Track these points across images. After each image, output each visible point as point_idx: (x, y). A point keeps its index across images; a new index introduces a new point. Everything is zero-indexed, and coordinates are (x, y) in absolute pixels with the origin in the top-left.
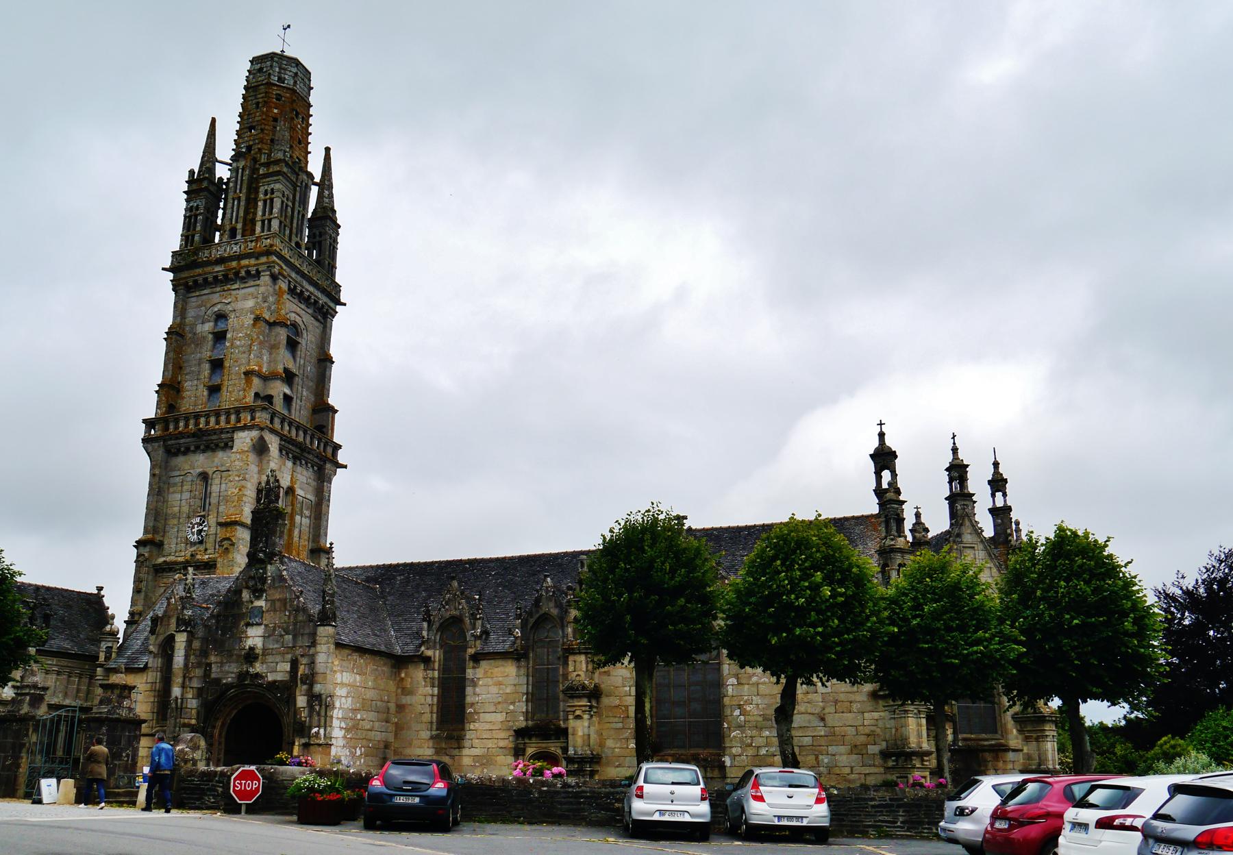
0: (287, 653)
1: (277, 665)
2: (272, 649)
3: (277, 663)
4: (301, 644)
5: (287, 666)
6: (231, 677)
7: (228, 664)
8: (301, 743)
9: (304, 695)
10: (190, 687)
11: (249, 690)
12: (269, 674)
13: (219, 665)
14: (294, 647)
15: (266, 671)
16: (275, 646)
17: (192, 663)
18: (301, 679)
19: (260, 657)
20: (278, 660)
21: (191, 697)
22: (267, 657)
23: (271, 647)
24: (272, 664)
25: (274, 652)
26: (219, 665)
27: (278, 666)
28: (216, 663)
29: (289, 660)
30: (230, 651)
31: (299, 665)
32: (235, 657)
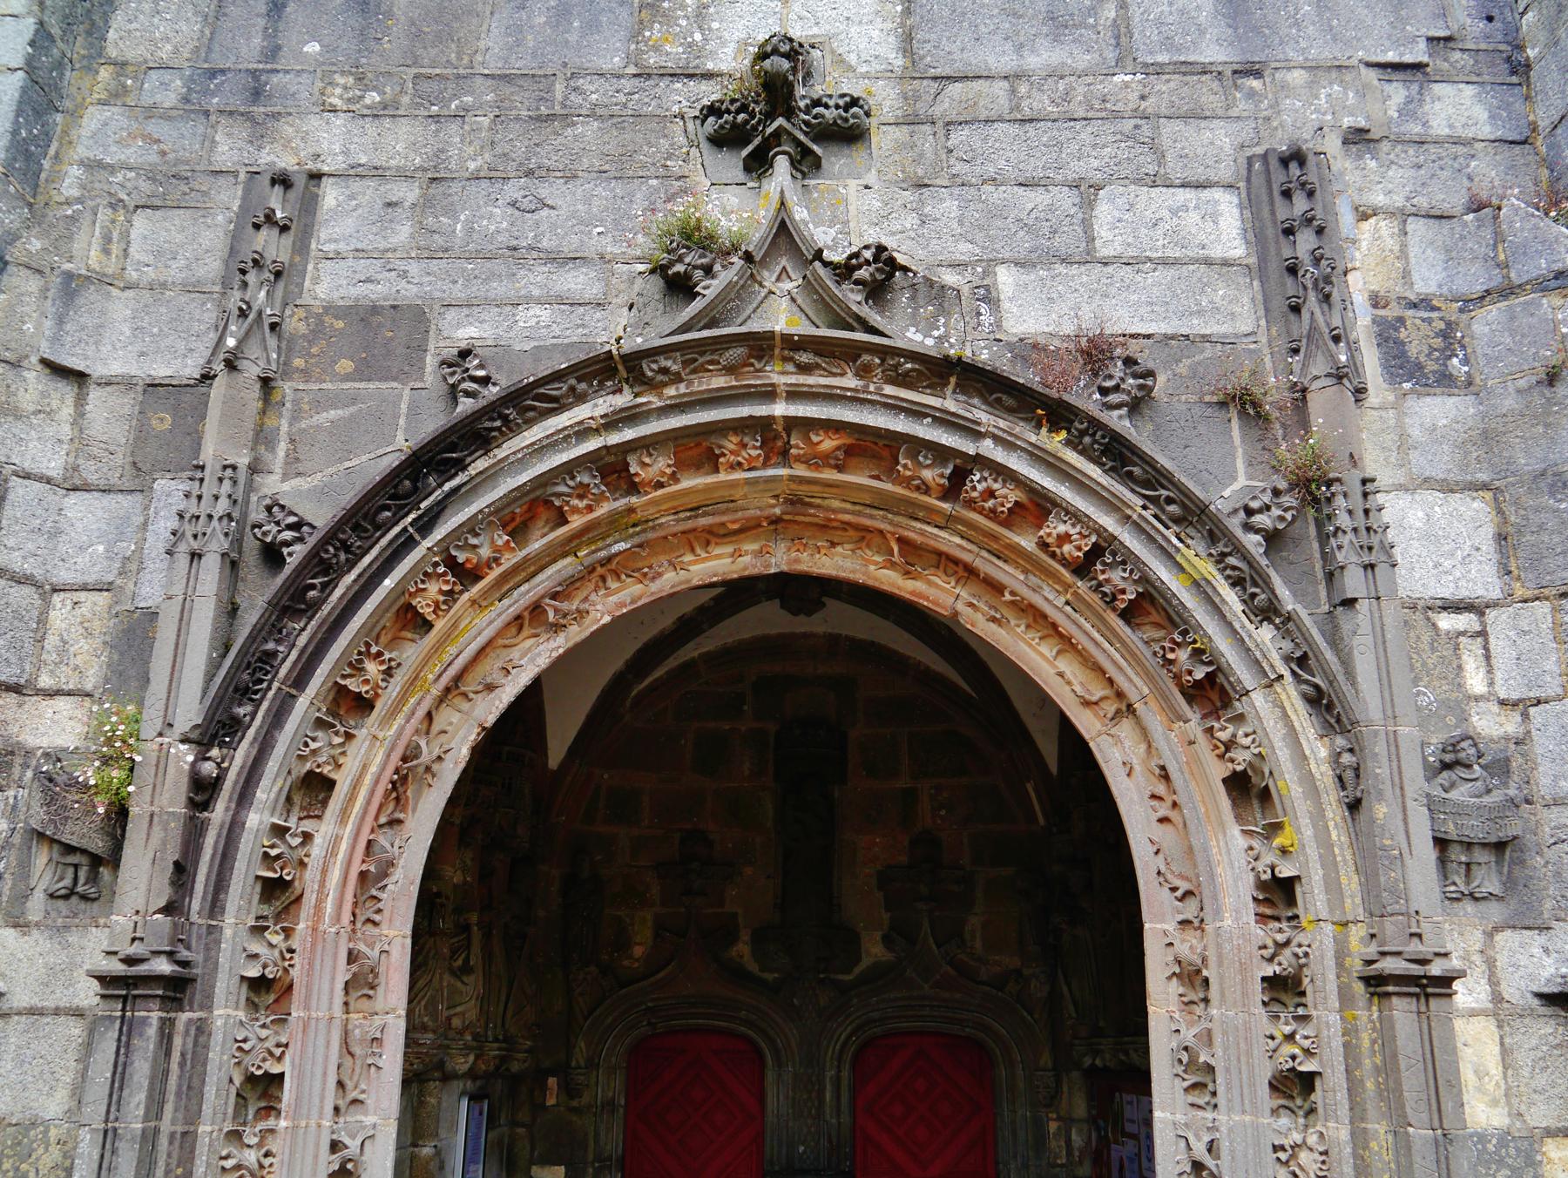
0: (1196, 115)
1: (1088, 204)
2: (1013, 77)
3: (1088, 191)
4: (1321, 51)
5: (1215, 217)
6: (560, 300)
7: (513, 190)
8: (1517, 989)
9: (1447, 488)
10: (58, 370)
11: (780, 409)
12: (1005, 278)
13: (409, 193)
14: (1252, 70)
15: (963, 250)
16: (1040, 58)
17: (93, 166)
18: (1388, 334)
19: (883, 139)
20: (1090, 167)
21: (54, 466)
22: (959, 136)
23: (1000, 59)
24: (1038, 198)
25: (1038, 102)
26: (409, 193)
27: (1105, 211)
28: (378, 173)
29: (1225, 172)
30: (540, 80)
31: (1346, 218)
32: (588, 130)
